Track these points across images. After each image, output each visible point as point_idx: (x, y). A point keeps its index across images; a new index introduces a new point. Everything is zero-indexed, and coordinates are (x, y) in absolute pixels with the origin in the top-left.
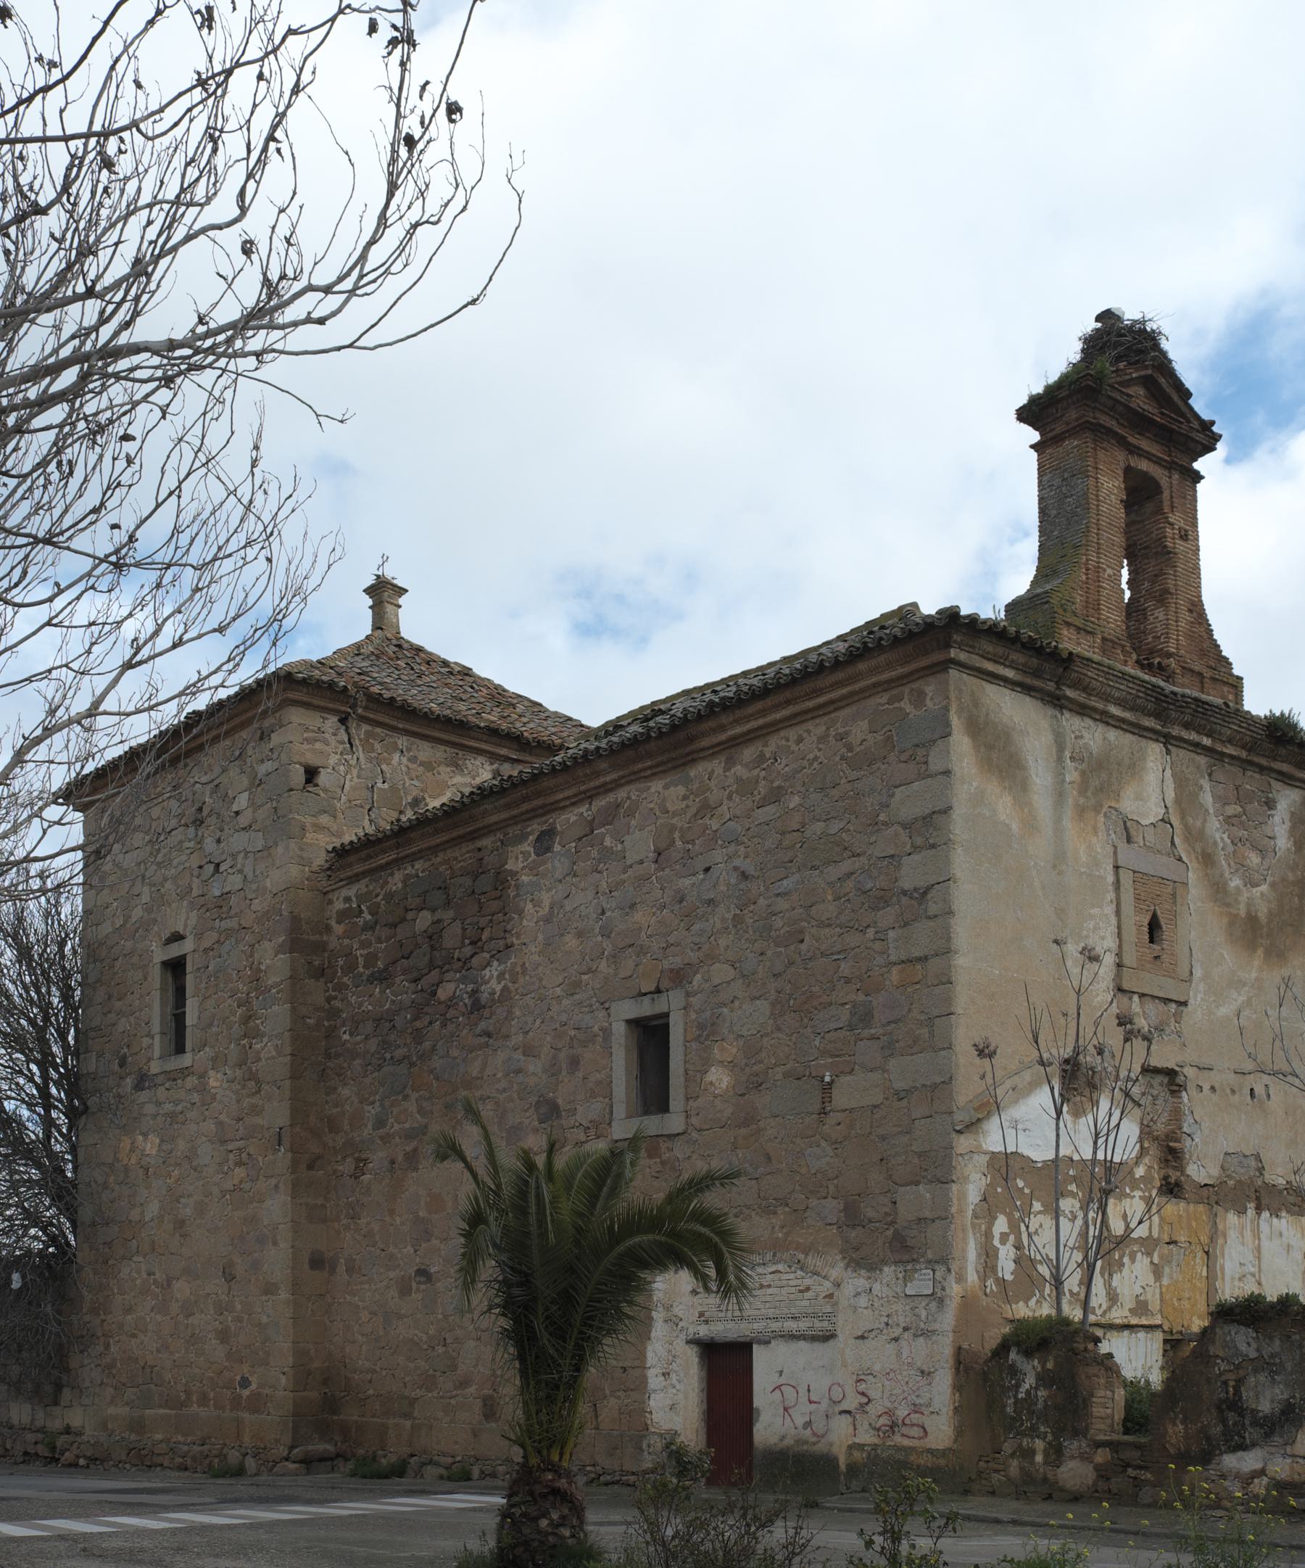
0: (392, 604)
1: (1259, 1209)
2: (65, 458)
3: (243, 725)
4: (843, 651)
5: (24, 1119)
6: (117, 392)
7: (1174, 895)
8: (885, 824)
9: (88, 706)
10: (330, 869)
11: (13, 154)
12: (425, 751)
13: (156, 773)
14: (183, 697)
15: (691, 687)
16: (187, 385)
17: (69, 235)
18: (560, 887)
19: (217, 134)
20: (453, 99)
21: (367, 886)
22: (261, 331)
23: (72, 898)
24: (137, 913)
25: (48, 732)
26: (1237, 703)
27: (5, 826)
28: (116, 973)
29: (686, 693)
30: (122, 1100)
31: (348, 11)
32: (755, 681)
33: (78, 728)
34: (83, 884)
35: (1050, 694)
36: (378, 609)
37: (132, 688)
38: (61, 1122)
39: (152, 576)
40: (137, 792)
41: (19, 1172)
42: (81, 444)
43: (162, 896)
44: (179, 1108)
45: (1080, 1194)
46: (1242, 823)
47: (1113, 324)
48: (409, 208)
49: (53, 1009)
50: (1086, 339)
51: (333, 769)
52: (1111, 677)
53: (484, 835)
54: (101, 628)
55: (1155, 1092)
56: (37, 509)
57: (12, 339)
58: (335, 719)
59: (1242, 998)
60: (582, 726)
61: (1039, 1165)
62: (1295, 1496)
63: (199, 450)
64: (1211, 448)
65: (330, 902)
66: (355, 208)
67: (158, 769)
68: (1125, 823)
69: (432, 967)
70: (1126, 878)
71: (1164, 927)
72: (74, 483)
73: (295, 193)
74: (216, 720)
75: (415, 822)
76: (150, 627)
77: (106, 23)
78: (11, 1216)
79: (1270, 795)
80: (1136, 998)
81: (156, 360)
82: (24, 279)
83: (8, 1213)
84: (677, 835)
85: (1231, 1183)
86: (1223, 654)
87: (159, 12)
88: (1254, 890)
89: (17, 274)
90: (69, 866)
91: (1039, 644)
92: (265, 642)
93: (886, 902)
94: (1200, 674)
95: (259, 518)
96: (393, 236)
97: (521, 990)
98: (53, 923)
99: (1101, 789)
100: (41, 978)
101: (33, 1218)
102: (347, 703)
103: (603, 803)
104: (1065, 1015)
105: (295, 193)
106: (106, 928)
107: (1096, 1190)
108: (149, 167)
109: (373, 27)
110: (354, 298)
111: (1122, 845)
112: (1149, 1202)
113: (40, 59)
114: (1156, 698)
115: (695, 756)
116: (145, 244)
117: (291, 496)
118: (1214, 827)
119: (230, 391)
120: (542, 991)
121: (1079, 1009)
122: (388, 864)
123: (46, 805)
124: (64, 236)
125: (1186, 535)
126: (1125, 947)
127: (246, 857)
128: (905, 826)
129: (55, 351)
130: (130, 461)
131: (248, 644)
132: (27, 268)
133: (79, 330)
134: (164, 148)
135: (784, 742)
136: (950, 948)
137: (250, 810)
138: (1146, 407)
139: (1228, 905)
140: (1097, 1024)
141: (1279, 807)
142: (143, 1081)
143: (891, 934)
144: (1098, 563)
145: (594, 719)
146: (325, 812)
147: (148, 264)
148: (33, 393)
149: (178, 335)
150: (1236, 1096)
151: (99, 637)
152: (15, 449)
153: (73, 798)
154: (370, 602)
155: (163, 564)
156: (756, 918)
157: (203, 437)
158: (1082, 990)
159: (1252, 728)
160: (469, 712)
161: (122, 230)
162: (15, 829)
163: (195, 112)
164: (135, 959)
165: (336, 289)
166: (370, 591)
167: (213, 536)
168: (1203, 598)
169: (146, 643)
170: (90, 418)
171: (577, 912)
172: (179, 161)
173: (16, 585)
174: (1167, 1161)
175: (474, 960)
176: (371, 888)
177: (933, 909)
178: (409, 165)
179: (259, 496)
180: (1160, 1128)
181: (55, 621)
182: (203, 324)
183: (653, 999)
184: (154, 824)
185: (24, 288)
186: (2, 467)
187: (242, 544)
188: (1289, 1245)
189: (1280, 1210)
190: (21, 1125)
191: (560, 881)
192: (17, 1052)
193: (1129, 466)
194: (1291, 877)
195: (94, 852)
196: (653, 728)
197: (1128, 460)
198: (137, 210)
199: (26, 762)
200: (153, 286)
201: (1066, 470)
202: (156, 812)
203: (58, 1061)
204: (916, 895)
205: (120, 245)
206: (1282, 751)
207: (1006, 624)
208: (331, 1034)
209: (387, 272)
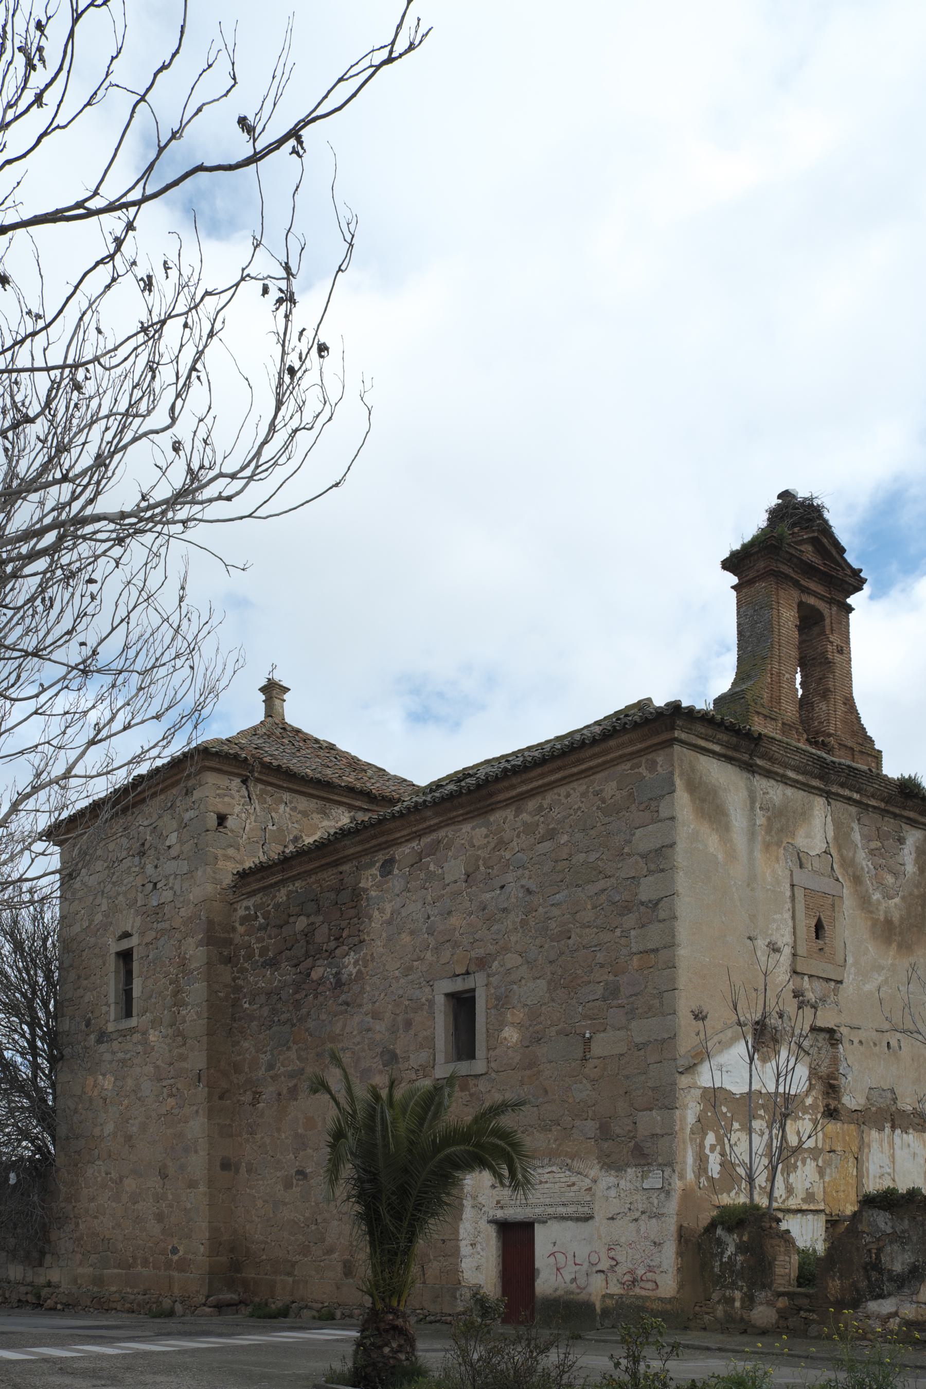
0: (279, 699)
1: (893, 1128)
2: (47, 596)
3: (173, 785)
4: (599, 732)
5: (18, 1064)
6: (84, 549)
7: (833, 905)
8: (629, 855)
9: (63, 771)
10: (235, 887)
11: (10, 380)
12: (303, 803)
13: (112, 818)
14: (131, 765)
15: (491, 757)
16: (133, 544)
17: (50, 438)
18: (398, 899)
19: (155, 366)
20: (322, 341)
21: (261, 899)
22: (186, 506)
23: (52, 907)
24: (99, 918)
25: (35, 789)
26: (878, 769)
27: (4, 857)
28: (83, 961)
29: (487, 762)
30: (88, 1050)
31: (248, 278)
32: (536, 754)
33: (56, 787)
34: (60, 897)
35: (745, 763)
36: (269, 702)
37: (95, 758)
38: (44, 1066)
39: (109, 679)
40: (98, 832)
41: (15, 1102)
42: (59, 585)
43: (116, 906)
44: (128, 1056)
45: (767, 1117)
46: (881, 854)
47: (790, 501)
48: (291, 418)
49: (39, 986)
50: (771, 511)
51: (237, 816)
52: (788, 751)
53: (344, 862)
54: (73, 716)
55: (820, 1045)
56: (27, 631)
57: (10, 511)
58: (239, 780)
59: (881, 979)
60: (414, 785)
61: (738, 1096)
62: (919, 1331)
63: (142, 590)
64: (859, 589)
65: (235, 910)
66: (253, 418)
67: (113, 816)
68: (798, 854)
69: (307, 955)
70: (799, 893)
71: (826, 928)
72: (54, 613)
73: (210, 408)
74: (154, 781)
75: (295, 854)
76: (108, 715)
77: (77, 287)
78: (9, 1133)
79: (902, 834)
80: (806, 978)
81: (112, 526)
82: (18, 469)
83: (7, 1130)
84: (481, 862)
85: (874, 1109)
86: (868, 734)
87: (114, 280)
88: (890, 902)
89: (13, 465)
90: (50, 885)
91: (737, 727)
92: (189, 726)
93: (629, 910)
94: (852, 749)
95: (185, 638)
96: (280, 438)
97: (370, 972)
98: (39, 925)
99: (781, 830)
100: (30, 964)
101: (25, 1134)
102: (247, 769)
103: (429, 840)
104: (756, 990)
105: (210, 408)
106: (76, 929)
107: (778, 1114)
108: (107, 389)
109: (265, 290)
110: (252, 482)
111: (796, 870)
112: (815, 1123)
113: (29, 313)
114: (820, 766)
115: (494, 806)
116: (104, 444)
117: (207, 622)
118: (862, 858)
119: (164, 548)
120: (386, 973)
121: (766, 986)
122: (276, 883)
123: (34, 841)
124: (46, 438)
125: (842, 650)
126: (799, 942)
127: (175, 878)
128: (643, 856)
129: (40, 520)
130: (93, 598)
131: (177, 727)
132: (20, 461)
133: (57, 505)
134: (117, 375)
135: (557, 797)
136: (674, 943)
137: (178, 845)
138: (813, 559)
139: (871, 912)
140: (778, 996)
141: (907, 843)
142: (102, 1037)
143: (633, 933)
144: (780, 669)
145: (422, 780)
146: (232, 846)
147: (106, 458)
148: (24, 550)
149: (128, 508)
150: (877, 1048)
151: (72, 722)
152: (12, 590)
153: (52, 836)
154: (263, 698)
155: (116, 670)
156: (537, 921)
157: (145, 580)
158: (768, 973)
159: (888, 787)
160: (333, 776)
161: (88, 434)
162: (12, 858)
163: (139, 350)
164: (97, 951)
165: (239, 476)
166: (263, 690)
167: (152, 650)
168: (854, 695)
169: (104, 726)
170: (65, 567)
171: (410, 918)
172: (128, 385)
173: (13, 685)
174: (828, 1093)
175: (337, 951)
176: (264, 900)
177: (662, 915)
178: (291, 387)
179: (185, 622)
180: (824, 1070)
181: (40, 711)
182: (145, 501)
183: (464, 979)
184: (110, 855)
185: (18, 475)
186: (2, 602)
187: (173, 656)
188: (914, 1153)
189: (908, 1128)
190: (16, 1067)
191: (398, 895)
192: (13, 1016)
193: (801, 600)
194: (916, 892)
195: (68, 875)
196: (464, 787)
197: (800, 597)
198: (98, 419)
199: (20, 811)
200: (109, 474)
201: (756, 604)
202: (111, 846)
203: (42, 1022)
204: (650, 905)
205: (86, 445)
206: (910, 803)
207: (714, 713)
208: (236, 1004)
209: (275, 464)
